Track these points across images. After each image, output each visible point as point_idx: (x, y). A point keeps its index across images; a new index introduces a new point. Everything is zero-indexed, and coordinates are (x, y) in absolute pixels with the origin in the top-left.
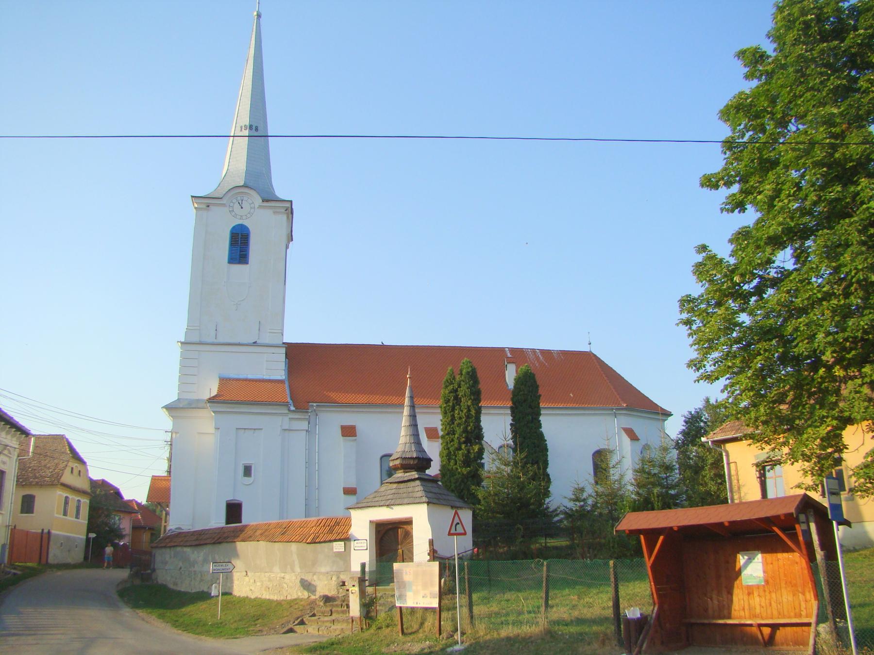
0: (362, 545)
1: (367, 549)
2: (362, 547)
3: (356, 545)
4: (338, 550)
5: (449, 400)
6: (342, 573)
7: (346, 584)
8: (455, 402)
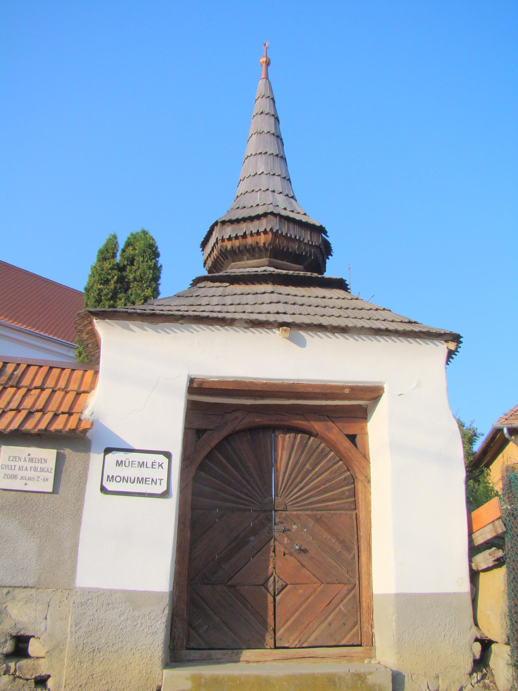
0: (143, 473)
1: (166, 494)
2: (141, 480)
3: (111, 470)
4: (18, 485)
5: (107, 282)
6: (20, 594)
7: (34, 648)
8: (119, 285)
